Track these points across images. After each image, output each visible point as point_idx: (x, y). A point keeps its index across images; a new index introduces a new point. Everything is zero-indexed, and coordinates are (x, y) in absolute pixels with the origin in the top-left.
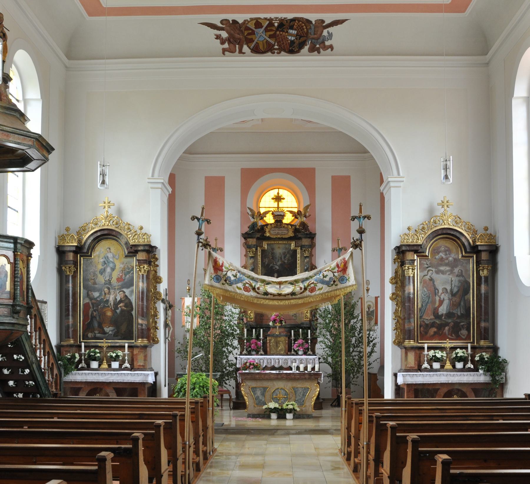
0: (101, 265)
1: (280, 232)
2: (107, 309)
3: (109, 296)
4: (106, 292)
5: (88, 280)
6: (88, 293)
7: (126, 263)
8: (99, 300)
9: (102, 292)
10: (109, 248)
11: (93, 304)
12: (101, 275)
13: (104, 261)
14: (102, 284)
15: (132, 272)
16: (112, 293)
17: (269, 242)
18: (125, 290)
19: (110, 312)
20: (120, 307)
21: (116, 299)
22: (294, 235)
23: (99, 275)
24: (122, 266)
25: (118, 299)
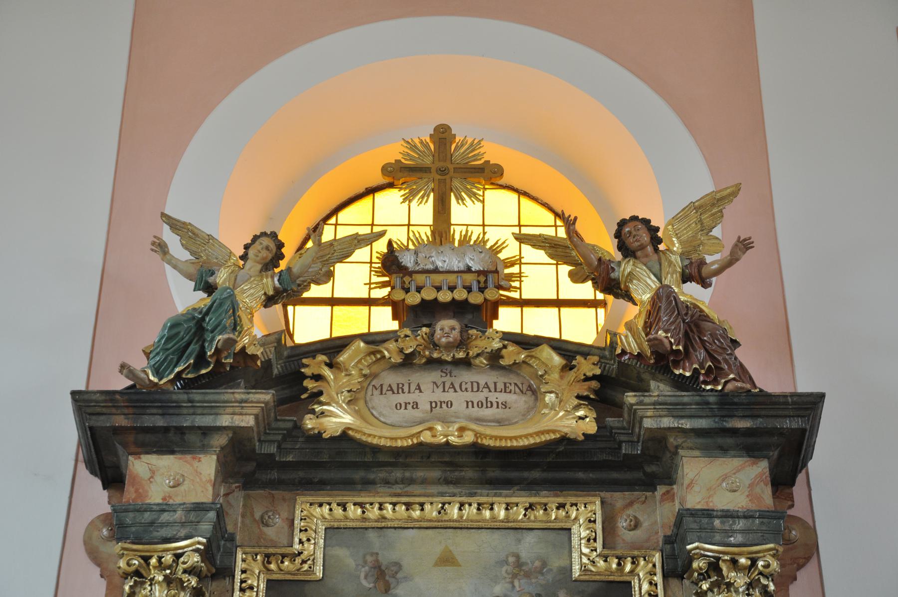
1: (459, 399)
17: (354, 512)
22: (590, 426)
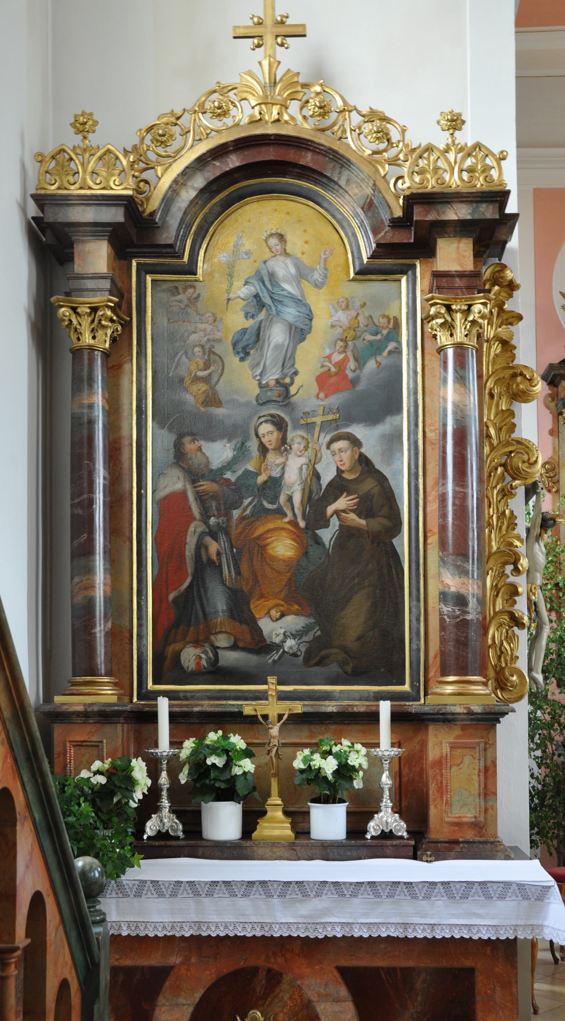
0: (241, 315)
2: (271, 526)
3: (280, 460)
4: (264, 440)
5: (182, 380)
6: (178, 448)
7: (364, 305)
8: (233, 479)
9: (246, 438)
10: (281, 237)
11: (201, 498)
12: (242, 359)
13: (257, 296)
14: (247, 404)
15: (391, 346)
16: (295, 446)
18: (358, 431)
19: (289, 542)
20: (337, 512)
21: (317, 476)
23: (233, 361)
24: (343, 317)
25: (328, 475)
